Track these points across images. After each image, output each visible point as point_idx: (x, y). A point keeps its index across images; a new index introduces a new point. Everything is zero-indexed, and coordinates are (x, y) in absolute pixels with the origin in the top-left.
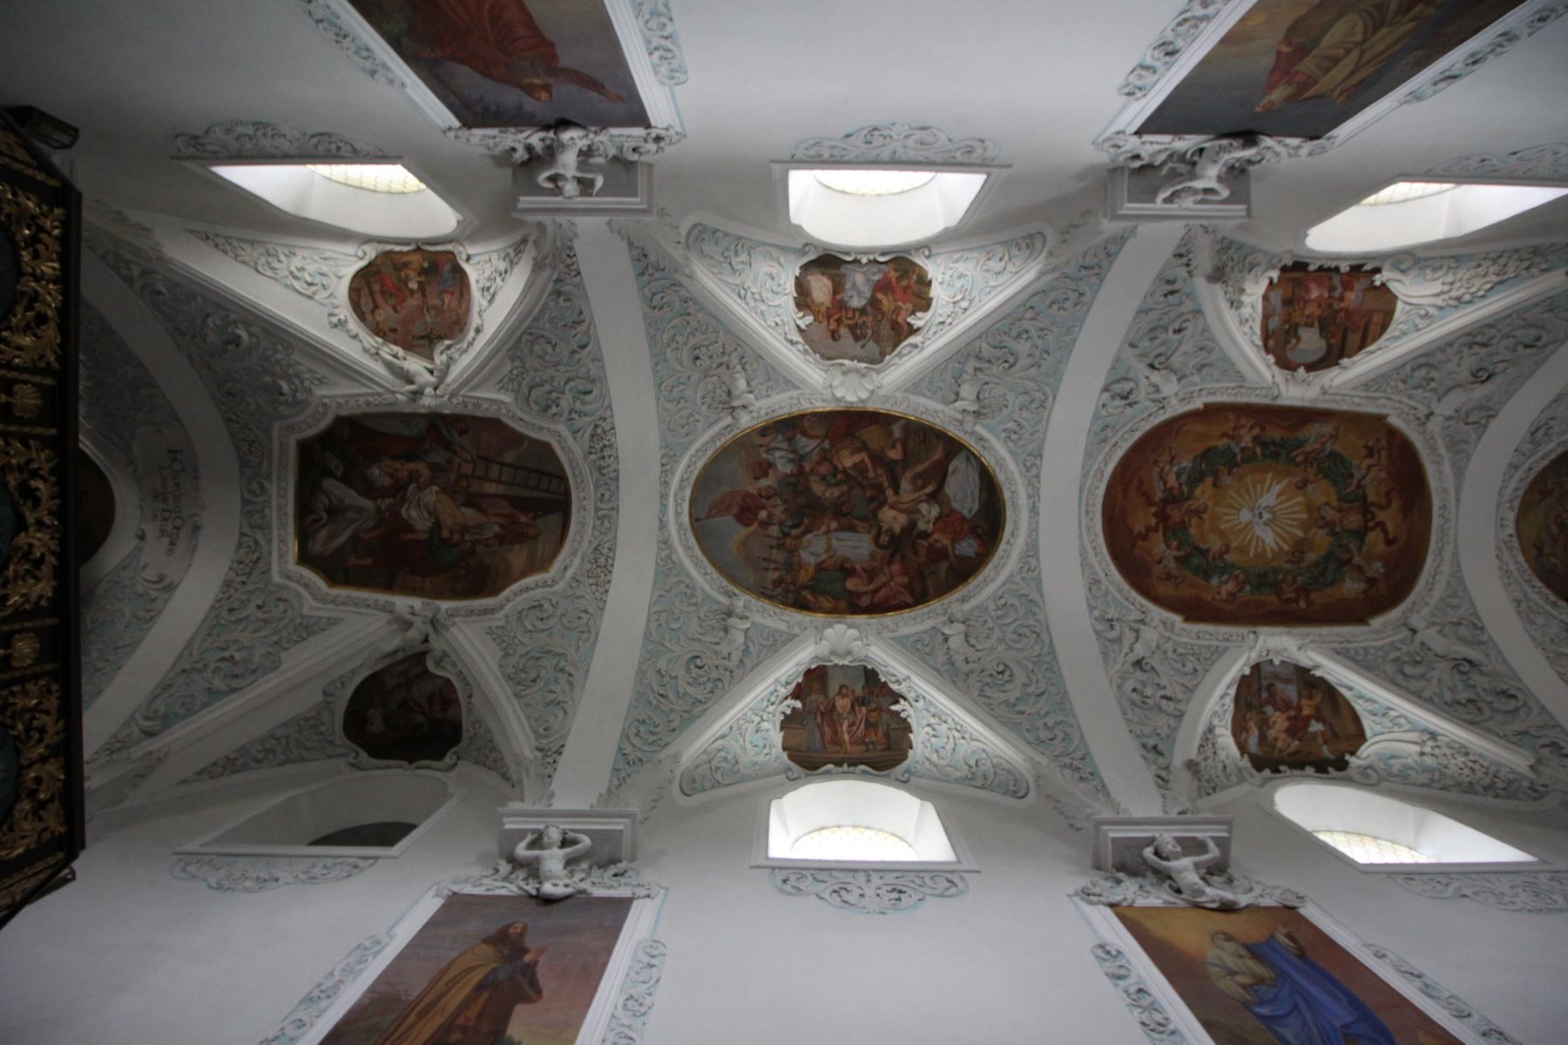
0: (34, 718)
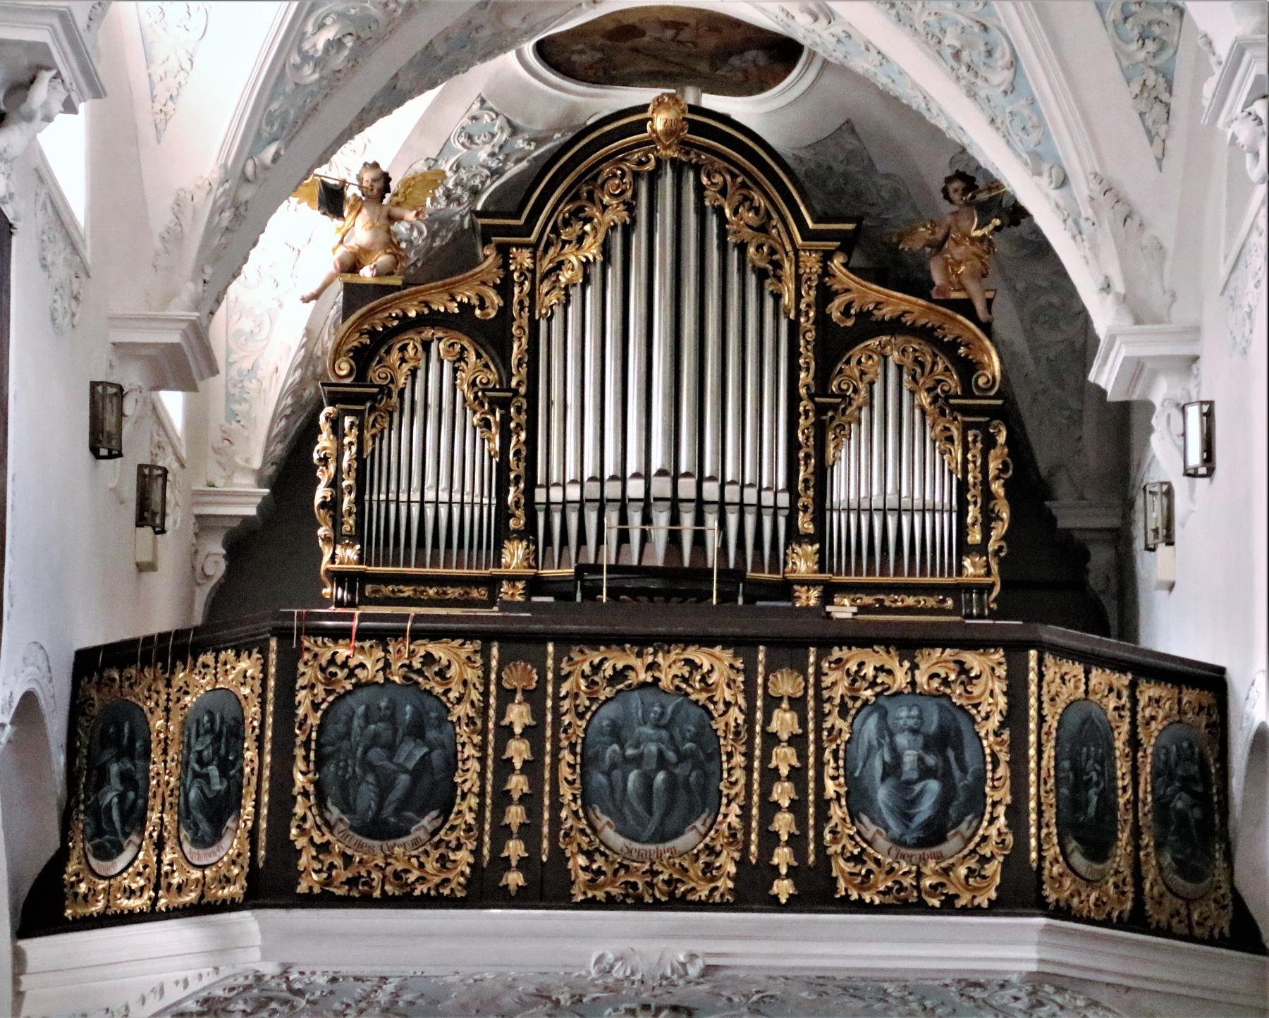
0: (864, 678)
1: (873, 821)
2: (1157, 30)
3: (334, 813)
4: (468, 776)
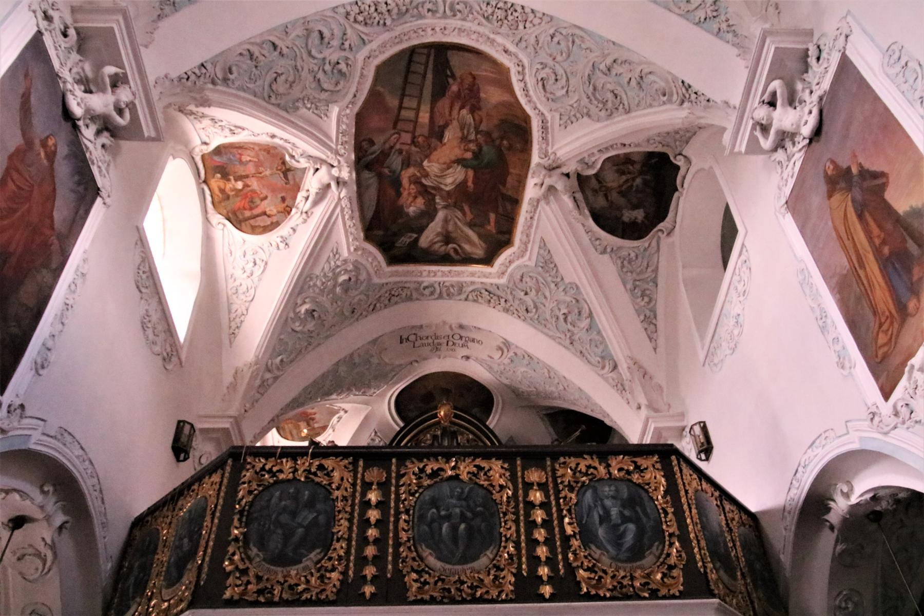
0: (580, 472)
1: (598, 548)
2: (648, 292)
3: (254, 551)
4: (341, 528)
